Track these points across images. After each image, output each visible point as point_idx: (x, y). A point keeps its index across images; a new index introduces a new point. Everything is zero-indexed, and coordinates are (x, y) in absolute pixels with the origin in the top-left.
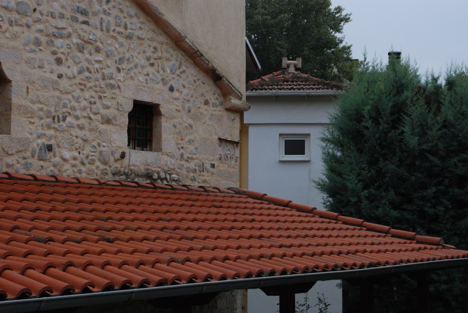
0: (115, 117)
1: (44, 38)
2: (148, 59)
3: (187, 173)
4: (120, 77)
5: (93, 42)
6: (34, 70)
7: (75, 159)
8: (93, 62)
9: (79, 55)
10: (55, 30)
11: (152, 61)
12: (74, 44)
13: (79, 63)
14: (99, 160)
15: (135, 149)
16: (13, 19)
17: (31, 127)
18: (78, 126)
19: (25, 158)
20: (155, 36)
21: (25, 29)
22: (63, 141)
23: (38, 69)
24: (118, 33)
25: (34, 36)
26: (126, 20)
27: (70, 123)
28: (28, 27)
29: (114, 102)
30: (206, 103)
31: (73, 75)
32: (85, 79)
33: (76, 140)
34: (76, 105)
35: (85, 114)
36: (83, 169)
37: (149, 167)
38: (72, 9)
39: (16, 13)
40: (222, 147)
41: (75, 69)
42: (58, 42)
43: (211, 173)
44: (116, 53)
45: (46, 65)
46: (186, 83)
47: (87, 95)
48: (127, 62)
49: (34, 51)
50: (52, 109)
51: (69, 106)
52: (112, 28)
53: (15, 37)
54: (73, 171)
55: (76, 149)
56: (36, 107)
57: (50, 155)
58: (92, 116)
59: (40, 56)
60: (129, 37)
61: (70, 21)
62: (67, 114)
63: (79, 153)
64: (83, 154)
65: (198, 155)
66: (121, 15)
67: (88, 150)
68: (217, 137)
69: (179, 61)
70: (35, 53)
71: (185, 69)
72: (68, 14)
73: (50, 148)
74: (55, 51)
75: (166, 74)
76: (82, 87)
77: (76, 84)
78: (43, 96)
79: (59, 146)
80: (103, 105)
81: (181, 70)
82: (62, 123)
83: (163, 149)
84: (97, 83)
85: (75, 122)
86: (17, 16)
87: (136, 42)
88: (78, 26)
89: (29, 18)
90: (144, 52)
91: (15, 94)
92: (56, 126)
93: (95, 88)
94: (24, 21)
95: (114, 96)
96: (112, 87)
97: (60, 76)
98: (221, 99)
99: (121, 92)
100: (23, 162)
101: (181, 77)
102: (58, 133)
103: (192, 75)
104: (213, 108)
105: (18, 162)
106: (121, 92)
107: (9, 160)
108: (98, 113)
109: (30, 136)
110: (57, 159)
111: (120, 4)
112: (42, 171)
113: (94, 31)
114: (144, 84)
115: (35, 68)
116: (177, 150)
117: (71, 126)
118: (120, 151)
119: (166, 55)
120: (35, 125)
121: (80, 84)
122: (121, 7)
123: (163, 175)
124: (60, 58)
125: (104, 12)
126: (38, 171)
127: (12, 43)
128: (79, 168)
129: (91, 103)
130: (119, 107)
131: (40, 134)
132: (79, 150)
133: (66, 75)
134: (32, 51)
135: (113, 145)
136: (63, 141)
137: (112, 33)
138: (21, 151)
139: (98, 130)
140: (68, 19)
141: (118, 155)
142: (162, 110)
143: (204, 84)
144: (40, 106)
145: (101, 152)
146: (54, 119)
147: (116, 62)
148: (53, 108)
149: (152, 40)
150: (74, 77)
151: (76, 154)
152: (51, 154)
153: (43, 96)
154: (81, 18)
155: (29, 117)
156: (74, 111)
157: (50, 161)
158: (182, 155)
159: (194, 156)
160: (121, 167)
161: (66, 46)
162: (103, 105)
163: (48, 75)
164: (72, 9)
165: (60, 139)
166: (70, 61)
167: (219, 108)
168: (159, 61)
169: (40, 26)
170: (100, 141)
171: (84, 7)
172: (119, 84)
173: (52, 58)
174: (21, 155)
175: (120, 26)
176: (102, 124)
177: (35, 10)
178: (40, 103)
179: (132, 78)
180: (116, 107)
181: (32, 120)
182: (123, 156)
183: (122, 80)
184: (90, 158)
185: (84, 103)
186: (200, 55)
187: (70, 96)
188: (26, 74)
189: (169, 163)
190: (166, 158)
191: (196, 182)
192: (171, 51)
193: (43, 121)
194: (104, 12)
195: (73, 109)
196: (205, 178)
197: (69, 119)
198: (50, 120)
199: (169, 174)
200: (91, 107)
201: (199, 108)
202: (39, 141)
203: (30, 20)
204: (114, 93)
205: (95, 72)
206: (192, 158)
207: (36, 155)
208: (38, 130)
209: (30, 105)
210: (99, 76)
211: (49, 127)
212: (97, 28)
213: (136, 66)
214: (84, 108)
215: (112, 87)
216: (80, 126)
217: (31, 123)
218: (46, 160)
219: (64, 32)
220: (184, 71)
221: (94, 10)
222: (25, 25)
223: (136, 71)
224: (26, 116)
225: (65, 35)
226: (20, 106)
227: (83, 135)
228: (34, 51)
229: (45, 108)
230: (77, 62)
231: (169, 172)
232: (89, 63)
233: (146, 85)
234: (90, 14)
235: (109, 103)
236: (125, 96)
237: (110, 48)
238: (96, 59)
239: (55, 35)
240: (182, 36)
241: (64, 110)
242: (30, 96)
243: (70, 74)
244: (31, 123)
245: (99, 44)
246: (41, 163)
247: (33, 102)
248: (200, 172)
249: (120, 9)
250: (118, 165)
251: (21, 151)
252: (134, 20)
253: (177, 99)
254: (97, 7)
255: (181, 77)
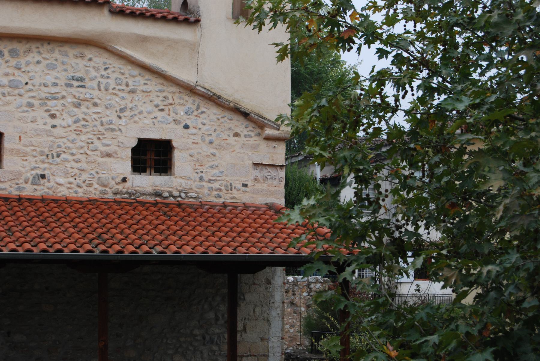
0: (116, 152)
1: (37, 101)
2: (157, 106)
3: (209, 192)
4: (123, 121)
5: (89, 100)
6: (27, 124)
7: (70, 183)
8: (91, 114)
9: (76, 110)
10: (48, 95)
11: (161, 107)
12: (69, 103)
13: (74, 116)
14: (98, 184)
15: (151, 175)
16: (6, 92)
17: (24, 163)
18: (74, 160)
19: (17, 184)
20: (165, 88)
21: (18, 98)
22: (57, 171)
23: (31, 123)
24: (119, 90)
25: (26, 101)
26: (127, 80)
27: (64, 159)
28: (20, 95)
29: (115, 141)
30: (236, 135)
31: (68, 124)
32: (81, 127)
33: (71, 170)
34: (71, 145)
35: (82, 151)
36: (79, 190)
37: (157, 188)
38: (66, 79)
39: (8, 88)
40: (258, 170)
41: (70, 121)
42: (50, 103)
43: (243, 191)
44: (116, 105)
45: (39, 119)
46: (205, 121)
47: (83, 137)
48: (130, 110)
49: (27, 111)
50: (46, 150)
51: (64, 147)
52: (111, 87)
53: (8, 103)
54: (69, 192)
55: (72, 177)
56: (28, 149)
57: (42, 181)
58: (88, 152)
59: (33, 114)
60: (133, 92)
61: (65, 88)
62: (62, 152)
63: (75, 179)
64: (80, 180)
65: (224, 178)
66: (122, 77)
67: (85, 176)
68: (251, 162)
69: (196, 104)
70: (28, 112)
71: (205, 110)
72: (62, 82)
73: (43, 176)
74: (48, 109)
75: (179, 116)
76: (78, 133)
77: (71, 131)
78: (36, 141)
79: (53, 175)
80: (102, 144)
81: (200, 111)
82: (55, 159)
83: (175, 173)
84: (95, 129)
85: (70, 158)
86: (10, 90)
87: (139, 95)
88: (73, 90)
89: (21, 90)
90: (151, 102)
91: (7, 141)
92: (50, 161)
93: (92, 133)
94: (16, 92)
95: (114, 137)
96: (113, 130)
97: (54, 126)
98: (259, 131)
99: (122, 133)
100: (16, 186)
101: (199, 117)
102: (52, 166)
103: (214, 114)
104: (245, 139)
105: (11, 187)
106: (122, 133)
107: (2, 186)
108: (96, 150)
109: (23, 169)
110: (52, 184)
111: (120, 69)
112: (36, 192)
113: (90, 92)
114: (151, 125)
115: (27, 123)
116: (196, 175)
117: (66, 160)
118: (122, 176)
119: (177, 101)
120: (28, 161)
121: (75, 130)
122: (122, 71)
123: (176, 193)
124: (54, 114)
125: (102, 76)
126: (32, 192)
127: (7, 108)
128: (75, 190)
129: (88, 143)
130: (120, 144)
131: (33, 168)
132: (75, 177)
133: (61, 125)
134: (24, 112)
135: (113, 172)
136: (57, 171)
137: (111, 91)
138: (14, 179)
139: (97, 162)
140: (62, 86)
141: (119, 179)
142: (174, 144)
143: (231, 120)
144: (33, 148)
145: (99, 178)
146: (47, 156)
147: (117, 112)
148: (47, 149)
149: (161, 91)
150: (69, 126)
151: (72, 180)
152: (45, 181)
153: (36, 141)
154: (76, 83)
155: (21, 156)
156: (69, 150)
157: (44, 186)
158: (201, 179)
159: (218, 178)
160: (123, 188)
161: (60, 105)
162: (102, 144)
163: (41, 126)
164: (66, 79)
165: (55, 170)
166: (65, 115)
167: (256, 138)
168: (170, 107)
169: (31, 94)
170: (98, 170)
171: (80, 75)
172: (120, 127)
173: (46, 115)
174: (14, 182)
175: (120, 85)
176: (102, 157)
177: (27, 84)
178: (34, 146)
179: (135, 122)
180: (117, 144)
181: (25, 158)
182: (124, 180)
183: (124, 124)
184: (87, 182)
185: (80, 144)
186: (217, 98)
187: (65, 140)
188: (19, 127)
189: (185, 184)
190: (180, 180)
191: (222, 198)
192: (186, 98)
193: (36, 159)
194: (102, 76)
195: (69, 148)
196: (234, 195)
197: (63, 156)
198: (44, 157)
199: (184, 193)
200: (88, 146)
201: (226, 139)
202: (34, 172)
203: (22, 91)
204: (114, 135)
205: (93, 121)
206: (216, 180)
207: (30, 182)
208: (31, 164)
209: (23, 148)
210: (98, 123)
211: (43, 162)
212: (94, 89)
213: (141, 113)
214: (80, 147)
215: (113, 130)
216: (76, 160)
217: (23, 160)
218: (40, 185)
219: (59, 96)
220: (203, 112)
221: (90, 76)
222: (17, 95)
223: (140, 116)
224: (19, 155)
225: (58, 97)
226: (12, 149)
227: (79, 166)
228: (27, 111)
229: (38, 149)
230: (72, 115)
231: (185, 191)
232: (85, 115)
233: (153, 126)
234: (87, 80)
235: (109, 142)
236: (127, 135)
237: (109, 102)
238: (93, 111)
239: (47, 99)
240: (192, 85)
241: (58, 150)
242: (22, 142)
243: (64, 123)
244: (23, 160)
245: (97, 101)
246: (35, 187)
247: (25, 146)
248: (228, 190)
249: (120, 72)
250: (120, 187)
251: (14, 179)
252: (139, 78)
253: (195, 134)
254: (93, 74)
255: (199, 117)
